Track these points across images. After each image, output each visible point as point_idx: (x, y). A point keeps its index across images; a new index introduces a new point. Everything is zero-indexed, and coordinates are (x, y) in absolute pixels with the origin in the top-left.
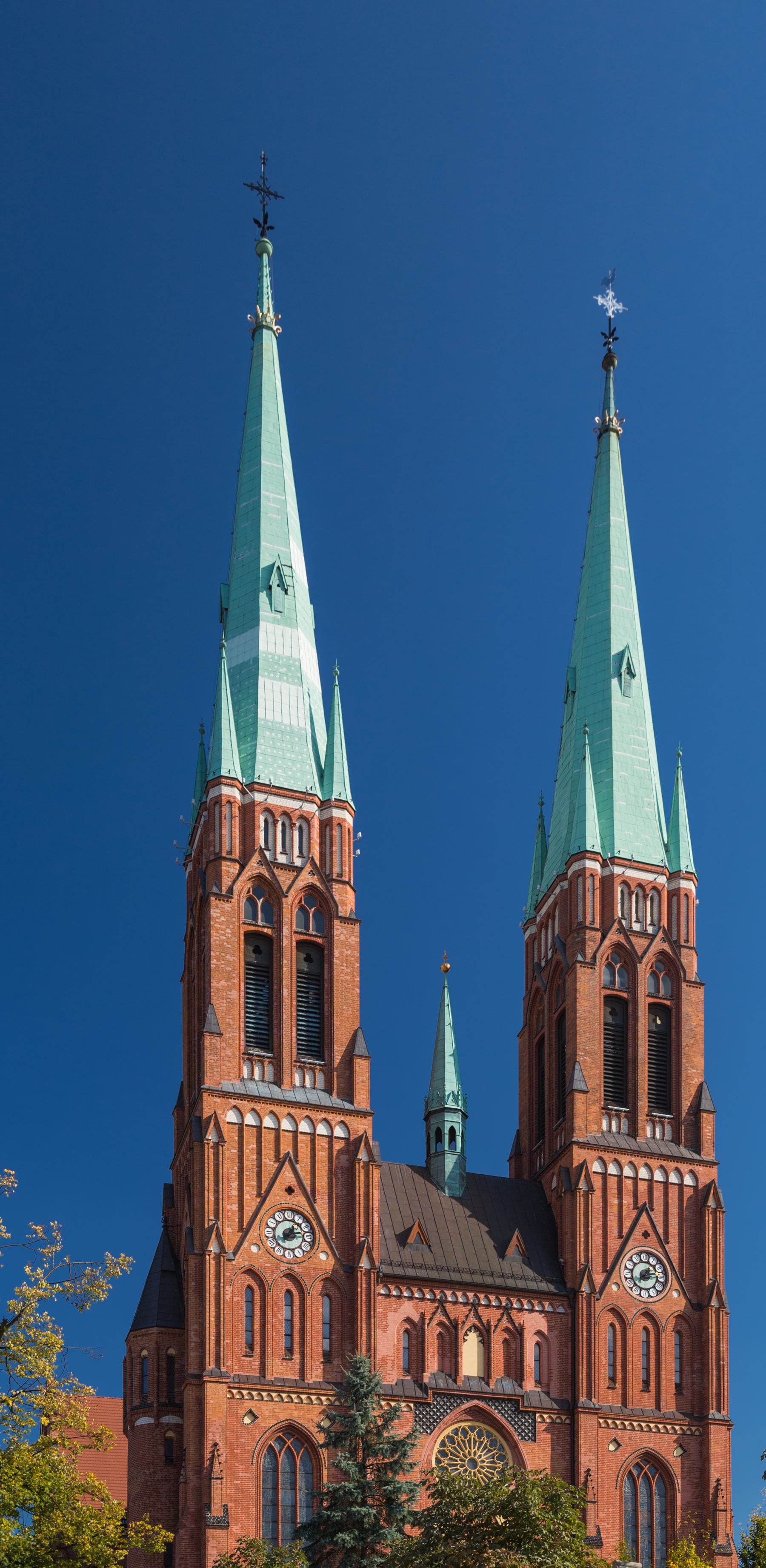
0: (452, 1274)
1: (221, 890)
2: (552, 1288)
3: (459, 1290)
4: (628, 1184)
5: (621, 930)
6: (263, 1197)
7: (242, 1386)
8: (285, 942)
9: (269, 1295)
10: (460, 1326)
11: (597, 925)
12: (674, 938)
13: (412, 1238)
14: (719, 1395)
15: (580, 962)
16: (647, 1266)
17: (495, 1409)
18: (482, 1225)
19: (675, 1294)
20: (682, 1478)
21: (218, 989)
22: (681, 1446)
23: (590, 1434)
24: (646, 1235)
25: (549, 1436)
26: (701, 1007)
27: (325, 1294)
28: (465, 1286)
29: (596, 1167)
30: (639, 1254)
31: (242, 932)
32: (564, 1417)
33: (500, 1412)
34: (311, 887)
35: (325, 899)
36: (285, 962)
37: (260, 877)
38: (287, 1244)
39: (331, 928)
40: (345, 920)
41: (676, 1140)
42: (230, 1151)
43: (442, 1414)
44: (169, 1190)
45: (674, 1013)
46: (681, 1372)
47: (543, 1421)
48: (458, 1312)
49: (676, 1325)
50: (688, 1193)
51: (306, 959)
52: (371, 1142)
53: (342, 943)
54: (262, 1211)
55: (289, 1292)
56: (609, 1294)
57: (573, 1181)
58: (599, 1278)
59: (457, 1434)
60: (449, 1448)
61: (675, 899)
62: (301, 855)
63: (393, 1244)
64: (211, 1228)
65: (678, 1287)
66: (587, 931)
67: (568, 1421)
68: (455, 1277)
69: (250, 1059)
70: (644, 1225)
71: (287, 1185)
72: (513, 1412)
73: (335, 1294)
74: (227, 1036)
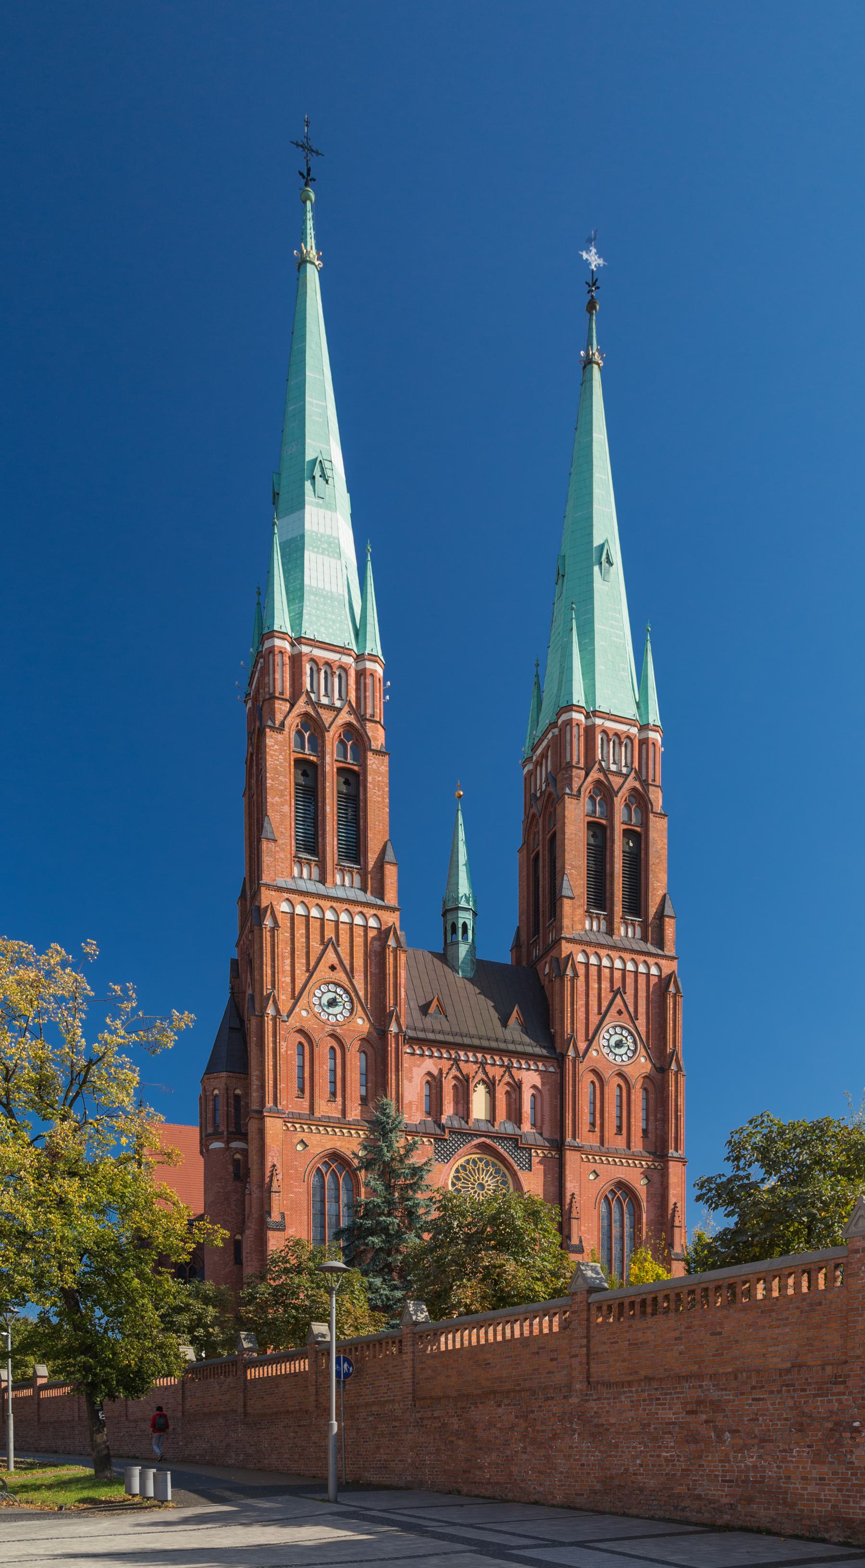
0: (465, 1039)
1: (274, 723)
2: (544, 1052)
3: (469, 1051)
4: (606, 972)
5: (601, 769)
6: (311, 972)
7: (295, 1120)
8: (328, 768)
9: (316, 1050)
11: (582, 765)
12: (644, 778)
13: (432, 1009)
14: (676, 1138)
15: (568, 794)
16: (621, 1037)
18: (488, 1001)
19: (643, 1060)
20: (647, 1202)
21: (273, 804)
22: (646, 1177)
24: (620, 1012)
25: (542, 1167)
26: (665, 834)
27: (362, 1051)
28: (475, 1048)
29: (580, 958)
30: (614, 1027)
31: (292, 758)
32: (554, 1153)
33: (503, 1147)
34: (349, 725)
35: (361, 735)
36: (327, 784)
37: (306, 714)
38: (331, 1010)
39: (365, 758)
40: (377, 752)
41: (644, 939)
42: (283, 935)
43: (456, 1148)
44: (234, 963)
45: (643, 838)
46: (647, 1120)
47: (537, 1155)
48: (469, 1069)
49: (643, 1083)
50: (654, 981)
51: (345, 783)
52: (398, 932)
53: (375, 771)
54: (310, 984)
55: (332, 1048)
56: (590, 1058)
57: (562, 968)
58: (582, 1046)
59: (468, 1164)
60: (462, 1174)
61: (644, 746)
62: (340, 698)
63: (417, 1014)
64: (269, 995)
65: (645, 1054)
66: (574, 770)
67: (557, 1156)
68: (467, 1041)
69: (300, 861)
70: (618, 1005)
71: (330, 964)
72: (513, 1148)
73: (370, 1051)
74: (280, 842)
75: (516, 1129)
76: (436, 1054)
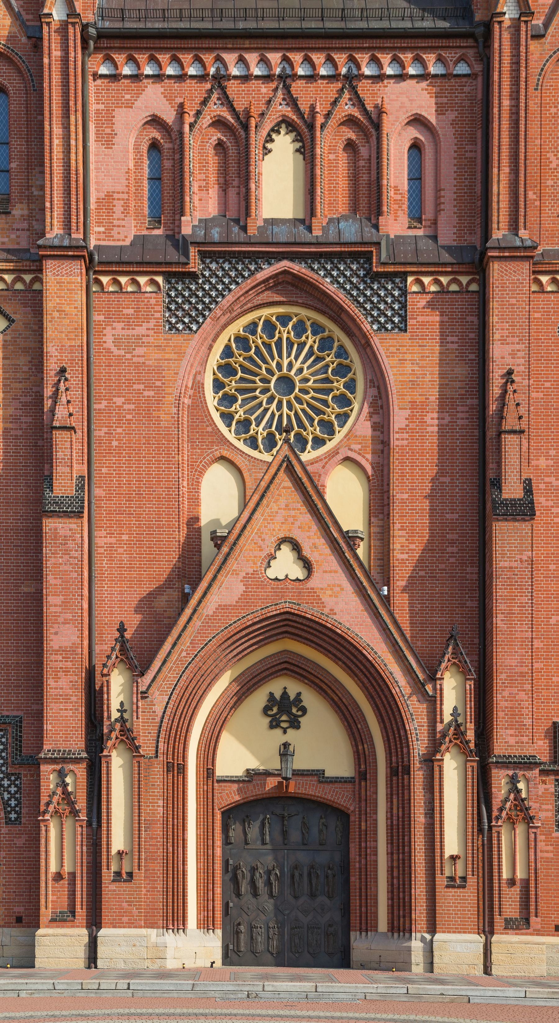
3: (249, 49)
10: (253, 122)
17: (325, 276)
33: (335, 280)
67: (474, 287)
76: (170, 71)
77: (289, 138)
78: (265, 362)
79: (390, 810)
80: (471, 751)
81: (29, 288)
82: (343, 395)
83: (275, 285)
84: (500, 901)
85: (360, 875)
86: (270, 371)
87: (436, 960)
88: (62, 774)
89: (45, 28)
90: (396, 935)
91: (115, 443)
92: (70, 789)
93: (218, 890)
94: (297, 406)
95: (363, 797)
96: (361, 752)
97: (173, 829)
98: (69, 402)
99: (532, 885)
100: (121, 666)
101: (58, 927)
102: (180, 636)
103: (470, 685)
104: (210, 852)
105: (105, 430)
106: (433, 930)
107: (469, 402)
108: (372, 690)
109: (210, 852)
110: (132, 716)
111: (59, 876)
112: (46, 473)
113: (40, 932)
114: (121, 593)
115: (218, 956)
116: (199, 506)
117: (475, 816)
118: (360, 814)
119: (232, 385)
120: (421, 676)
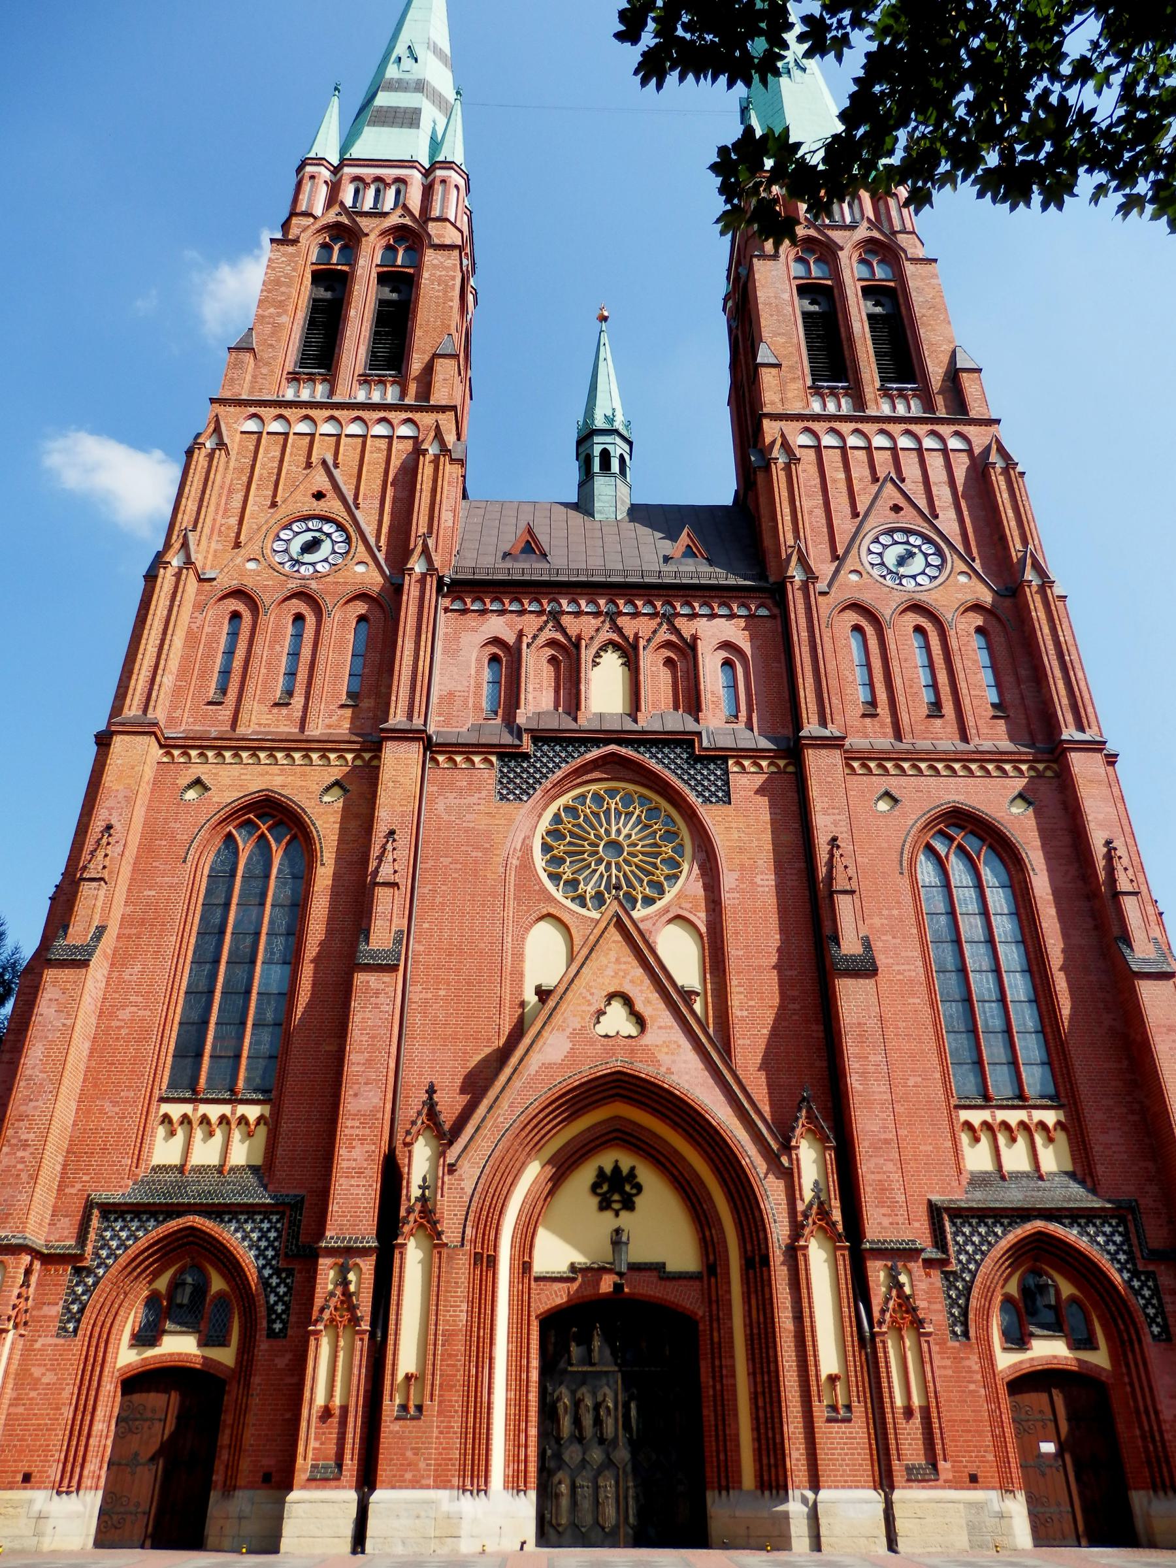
10: (583, 643)
23: (830, 779)
32: (782, 763)
33: (660, 761)
65: (965, 569)
75: (689, 719)
77: (615, 656)
78: (594, 828)
79: (748, 1314)
80: (840, 1235)
81: (367, 764)
82: (672, 858)
83: (604, 765)
84: (896, 1439)
85: (715, 1406)
86: (597, 836)
87: (823, 1531)
88: (343, 1271)
89: (407, 577)
90: (767, 1493)
91: (438, 900)
92: (352, 1288)
93: (533, 1432)
94: (627, 868)
95: (714, 1298)
96: (708, 1238)
97: (478, 1342)
98: (394, 860)
99: (934, 1414)
100: (428, 1133)
101: (317, 1488)
102: (498, 1097)
103: (830, 1155)
104: (524, 1376)
105: (430, 887)
106: (815, 1487)
107: (796, 865)
108: (717, 1162)
109: (524, 1376)
110: (436, 1193)
111: (326, 1413)
112: (364, 926)
113: (293, 1496)
114: (433, 1052)
115: (529, 1530)
116: (522, 961)
117: (853, 1319)
118: (711, 1321)
119: (560, 848)
120: (775, 1146)
